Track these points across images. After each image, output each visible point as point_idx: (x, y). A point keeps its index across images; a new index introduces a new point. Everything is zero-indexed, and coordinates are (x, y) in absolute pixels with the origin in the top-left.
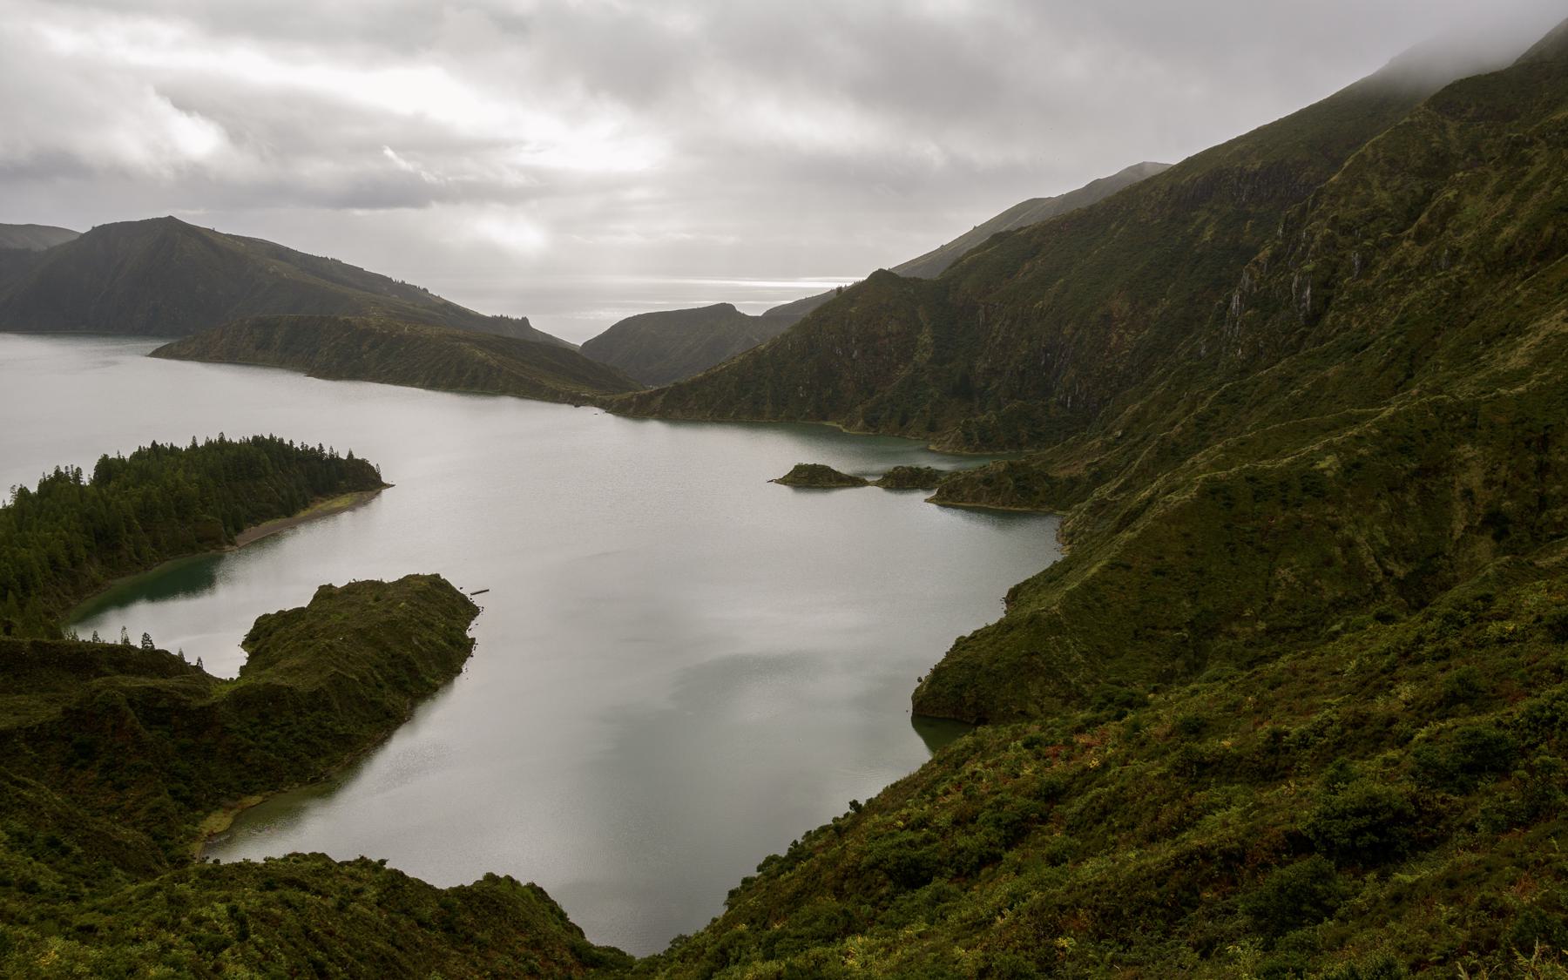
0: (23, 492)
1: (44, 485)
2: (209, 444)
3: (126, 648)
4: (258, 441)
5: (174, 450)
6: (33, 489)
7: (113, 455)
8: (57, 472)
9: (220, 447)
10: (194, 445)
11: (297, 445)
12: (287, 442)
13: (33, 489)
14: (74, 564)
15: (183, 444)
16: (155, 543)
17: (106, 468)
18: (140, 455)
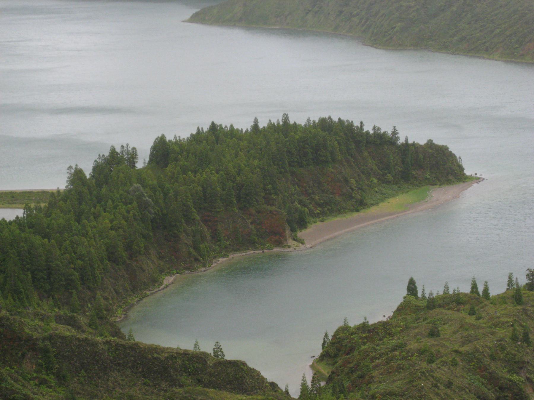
0: (77, 176)
1: (97, 168)
2: (271, 126)
3: (199, 358)
4: (325, 124)
5: (233, 133)
6: (88, 172)
7: (169, 137)
8: (113, 151)
9: (285, 128)
10: (255, 127)
11: (368, 128)
12: (357, 124)
13: (88, 172)
14: (131, 257)
15: (244, 125)
16: (216, 237)
17: (162, 151)
18: (197, 138)
